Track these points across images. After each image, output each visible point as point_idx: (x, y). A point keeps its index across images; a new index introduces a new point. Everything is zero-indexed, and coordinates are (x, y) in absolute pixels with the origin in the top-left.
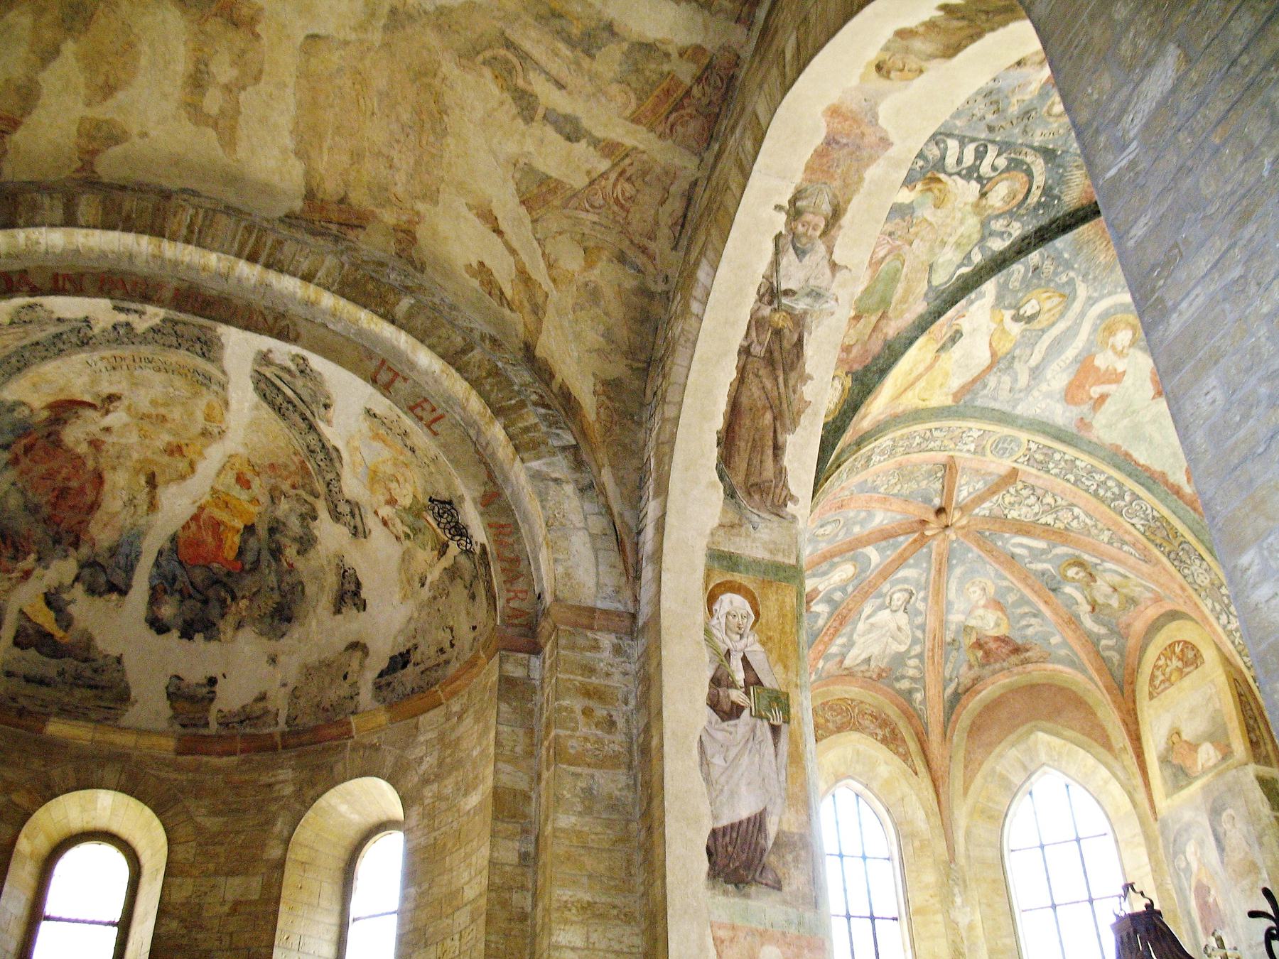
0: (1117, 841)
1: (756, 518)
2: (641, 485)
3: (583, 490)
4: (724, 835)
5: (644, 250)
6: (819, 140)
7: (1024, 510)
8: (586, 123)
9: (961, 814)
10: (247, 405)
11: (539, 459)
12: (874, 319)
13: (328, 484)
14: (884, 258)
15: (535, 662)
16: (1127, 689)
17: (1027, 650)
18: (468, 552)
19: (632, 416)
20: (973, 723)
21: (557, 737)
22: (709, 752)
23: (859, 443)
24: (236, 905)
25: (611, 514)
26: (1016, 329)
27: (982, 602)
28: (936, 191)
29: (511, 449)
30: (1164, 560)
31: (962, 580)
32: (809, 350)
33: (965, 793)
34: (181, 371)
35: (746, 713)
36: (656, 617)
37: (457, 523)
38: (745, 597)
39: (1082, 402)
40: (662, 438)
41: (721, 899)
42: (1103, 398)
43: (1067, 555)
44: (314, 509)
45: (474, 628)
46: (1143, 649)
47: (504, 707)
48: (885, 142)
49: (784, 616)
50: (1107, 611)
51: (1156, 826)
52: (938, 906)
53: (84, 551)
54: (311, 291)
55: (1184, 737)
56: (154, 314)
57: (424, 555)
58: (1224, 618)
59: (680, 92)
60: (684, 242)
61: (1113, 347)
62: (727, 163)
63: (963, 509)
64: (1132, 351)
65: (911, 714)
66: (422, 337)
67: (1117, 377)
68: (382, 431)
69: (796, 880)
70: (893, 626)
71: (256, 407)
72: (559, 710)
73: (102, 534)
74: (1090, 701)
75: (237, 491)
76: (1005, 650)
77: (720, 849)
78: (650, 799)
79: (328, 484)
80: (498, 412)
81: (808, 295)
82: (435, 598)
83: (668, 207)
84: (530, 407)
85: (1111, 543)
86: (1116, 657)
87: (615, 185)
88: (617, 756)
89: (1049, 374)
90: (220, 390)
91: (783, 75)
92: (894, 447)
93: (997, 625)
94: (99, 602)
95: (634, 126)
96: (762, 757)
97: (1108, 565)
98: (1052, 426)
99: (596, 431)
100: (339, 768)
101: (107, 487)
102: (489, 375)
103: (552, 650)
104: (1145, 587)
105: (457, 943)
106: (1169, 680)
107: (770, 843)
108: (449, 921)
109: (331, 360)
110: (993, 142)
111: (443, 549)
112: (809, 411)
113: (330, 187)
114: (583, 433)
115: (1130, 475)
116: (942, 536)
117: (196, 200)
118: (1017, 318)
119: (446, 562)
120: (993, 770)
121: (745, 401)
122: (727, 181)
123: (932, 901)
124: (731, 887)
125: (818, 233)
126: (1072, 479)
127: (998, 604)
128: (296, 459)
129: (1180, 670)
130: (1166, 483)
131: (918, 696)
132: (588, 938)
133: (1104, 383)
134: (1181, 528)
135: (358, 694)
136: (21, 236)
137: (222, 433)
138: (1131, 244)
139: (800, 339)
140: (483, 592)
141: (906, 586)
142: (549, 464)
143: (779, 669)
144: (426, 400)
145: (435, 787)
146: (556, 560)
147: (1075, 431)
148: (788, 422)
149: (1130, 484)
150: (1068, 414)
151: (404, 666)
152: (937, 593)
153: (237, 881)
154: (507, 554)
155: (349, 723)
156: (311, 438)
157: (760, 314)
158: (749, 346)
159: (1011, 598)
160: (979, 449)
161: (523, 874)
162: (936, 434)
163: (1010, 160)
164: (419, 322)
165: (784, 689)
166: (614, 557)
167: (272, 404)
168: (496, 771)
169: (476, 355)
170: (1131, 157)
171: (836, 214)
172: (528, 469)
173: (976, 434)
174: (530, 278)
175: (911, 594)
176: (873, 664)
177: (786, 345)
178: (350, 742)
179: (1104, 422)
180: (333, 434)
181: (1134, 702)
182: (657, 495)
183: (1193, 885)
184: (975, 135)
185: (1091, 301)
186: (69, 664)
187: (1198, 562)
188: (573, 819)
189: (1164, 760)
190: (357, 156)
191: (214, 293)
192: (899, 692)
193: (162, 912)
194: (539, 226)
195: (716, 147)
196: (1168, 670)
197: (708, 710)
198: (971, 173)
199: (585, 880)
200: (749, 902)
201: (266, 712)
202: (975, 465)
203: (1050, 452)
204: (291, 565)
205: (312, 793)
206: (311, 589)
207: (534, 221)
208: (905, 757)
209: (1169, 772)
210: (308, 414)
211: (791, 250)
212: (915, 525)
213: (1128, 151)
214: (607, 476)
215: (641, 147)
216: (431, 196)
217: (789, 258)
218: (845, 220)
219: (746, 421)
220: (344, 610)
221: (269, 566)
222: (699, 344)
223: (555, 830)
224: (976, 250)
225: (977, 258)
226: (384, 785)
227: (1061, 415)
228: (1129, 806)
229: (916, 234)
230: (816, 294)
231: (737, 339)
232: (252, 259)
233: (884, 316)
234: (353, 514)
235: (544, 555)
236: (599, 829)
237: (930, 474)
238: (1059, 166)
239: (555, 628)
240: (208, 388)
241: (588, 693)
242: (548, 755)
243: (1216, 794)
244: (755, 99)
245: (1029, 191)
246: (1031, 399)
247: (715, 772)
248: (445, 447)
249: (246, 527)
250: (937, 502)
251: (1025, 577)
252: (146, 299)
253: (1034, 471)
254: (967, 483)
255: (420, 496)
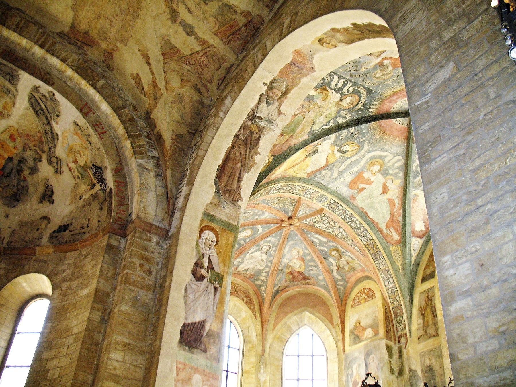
0: (327, 359)
1: (225, 203)
2: (181, 179)
3: (157, 176)
4: (188, 327)
5: (205, 86)
6: (288, 62)
7: (322, 225)
8: (196, 30)
9: (270, 338)
10: (23, 106)
11: (143, 159)
12: (287, 137)
13: (50, 148)
14: (297, 114)
15: (123, 241)
16: (344, 302)
17: (309, 279)
18: (103, 190)
19: (184, 151)
20: (282, 303)
21: (127, 273)
22: (188, 292)
23: (268, 184)
25: (167, 188)
26: (338, 155)
27: (297, 257)
28: (324, 94)
29: (132, 152)
30: (370, 256)
31: (291, 247)
32: (261, 143)
33: (273, 329)
35: (206, 280)
36: (178, 233)
37: (102, 177)
38: (214, 234)
39: (355, 189)
40: (195, 163)
41: (182, 352)
42: (363, 189)
43: (333, 246)
44: (41, 157)
45: (99, 221)
46: (353, 288)
47: (106, 256)
48: (313, 69)
49: (228, 244)
50: (343, 271)
51: (343, 356)
52: (254, 371)
54: (64, 67)
55: (362, 324)
57: (84, 187)
58: (387, 283)
59: (237, 28)
60: (221, 88)
61: (372, 171)
62: (248, 61)
63: (299, 219)
64: (378, 174)
65: (259, 295)
66: (106, 98)
67: (369, 182)
68: (79, 132)
69: (212, 350)
70: (260, 259)
71: (27, 109)
72: (130, 262)
74: (329, 304)
76: (301, 277)
77: (185, 332)
78: (161, 306)
79: (50, 148)
80: (130, 136)
81: (267, 121)
82: (84, 206)
83: (219, 72)
84: (143, 137)
85: (351, 245)
86: (342, 289)
87: (200, 58)
88: (150, 286)
89: (345, 175)
90: (13, 97)
91: (281, 33)
92: (280, 189)
93: (300, 267)
95: (215, 36)
96: (209, 298)
97: (348, 253)
98: (341, 195)
99: (168, 155)
100: (27, 267)
102: (129, 120)
103: (132, 238)
104: (360, 265)
105: (66, 350)
106: (360, 302)
107: (205, 333)
108: (64, 340)
109: (64, 96)
110: (351, 81)
111: (93, 186)
112: (255, 166)
113: (83, 26)
114: (163, 153)
115: (365, 221)
116: (288, 228)
117: (22, 15)
118: (339, 151)
119: (93, 192)
120: (285, 323)
121: (232, 156)
122: (246, 68)
123: (252, 369)
124: (187, 348)
125: (277, 98)
126: (343, 217)
127: (302, 259)
128: (39, 135)
129: (365, 299)
130: (378, 227)
131: (263, 288)
132: (124, 357)
133: (364, 184)
134: (379, 245)
135: (42, 238)
137: (8, 116)
138: (421, 131)
139: (259, 137)
140: (107, 208)
141: (269, 244)
142: (146, 162)
143: (221, 265)
144: (100, 124)
145: (68, 283)
146: (141, 201)
147: (349, 199)
148: (246, 169)
149: (364, 224)
150: (348, 192)
151: (65, 231)
152: (281, 249)
154: (120, 194)
155: (35, 250)
156: (48, 128)
157: (246, 123)
158: (239, 135)
159: (308, 258)
160: (311, 197)
161: (101, 326)
162: (297, 187)
163: (355, 90)
164: (106, 91)
165: (222, 274)
166: (164, 205)
167: (34, 109)
168: (98, 282)
169: (126, 111)
170: (427, 99)
171: (286, 92)
172: (137, 162)
173: (312, 191)
174: (157, 85)
175: (270, 247)
176: (248, 272)
177: (253, 138)
178: (34, 257)
179: (361, 198)
180: (57, 128)
181: (345, 308)
182: (188, 185)
183: (353, 381)
184: (345, 76)
185: (369, 151)
187: (382, 259)
188: (127, 308)
189: (352, 332)
190: (98, 16)
191: (21, 56)
192: (256, 285)
194: (166, 65)
195: (245, 53)
196: (361, 298)
197: (191, 275)
198: (339, 91)
199: (127, 333)
200: (193, 355)
202: (308, 203)
203: (338, 205)
204: (25, 178)
205: (12, 276)
206: (31, 190)
207: (164, 63)
208: (253, 311)
209: (352, 337)
210: (49, 117)
211: (265, 102)
212: (279, 221)
213: (427, 97)
214: (169, 173)
215: (215, 45)
216: (124, 41)
217: (263, 105)
218: (289, 96)
219: (231, 164)
220: (44, 202)
221: (15, 176)
222: (220, 129)
223: (119, 311)
224: (332, 120)
225: (332, 124)
226: (45, 278)
227: (345, 192)
228: (335, 347)
229: (312, 109)
230: (270, 121)
231: (235, 131)
232: (42, 46)
233: (291, 137)
234: (57, 163)
235: (136, 198)
236: (137, 314)
237: (291, 202)
238: (372, 97)
239: (135, 229)
240: (8, 95)
241: (143, 258)
242: (122, 280)
243: (369, 348)
244: (266, 39)
245: (358, 103)
246: (336, 183)
247: (189, 301)
248: (104, 145)
249: (9, 157)
250: (290, 214)
251: (315, 251)
253: (330, 211)
254: (303, 210)
255: (88, 163)
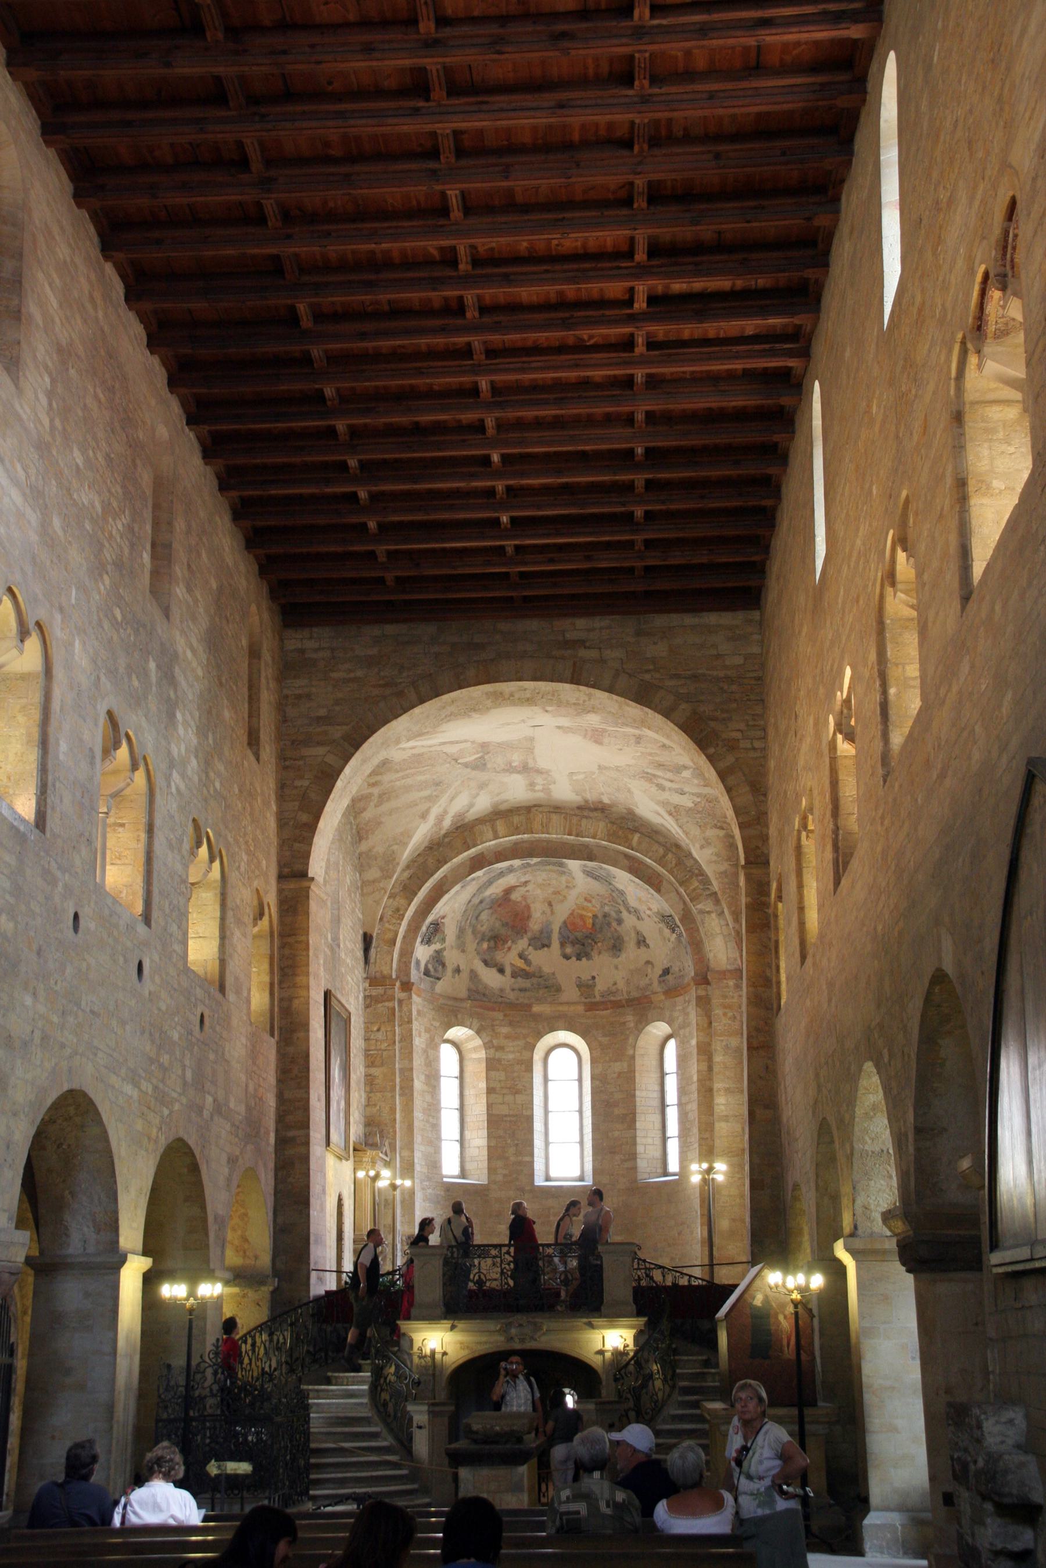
24: (620, 1074)
34: (550, 871)
53: (529, 934)
56: (535, 860)
73: (535, 925)
75: (586, 904)
80: (681, 884)
94: (539, 952)
101: (532, 909)
117: (540, 809)
136: (480, 847)
153: (619, 1063)
169: (670, 855)
180: (621, 887)
186: (535, 980)
193: (592, 1078)
201: (618, 990)
206: (626, 938)
232: (570, 834)
252: (531, 855)
